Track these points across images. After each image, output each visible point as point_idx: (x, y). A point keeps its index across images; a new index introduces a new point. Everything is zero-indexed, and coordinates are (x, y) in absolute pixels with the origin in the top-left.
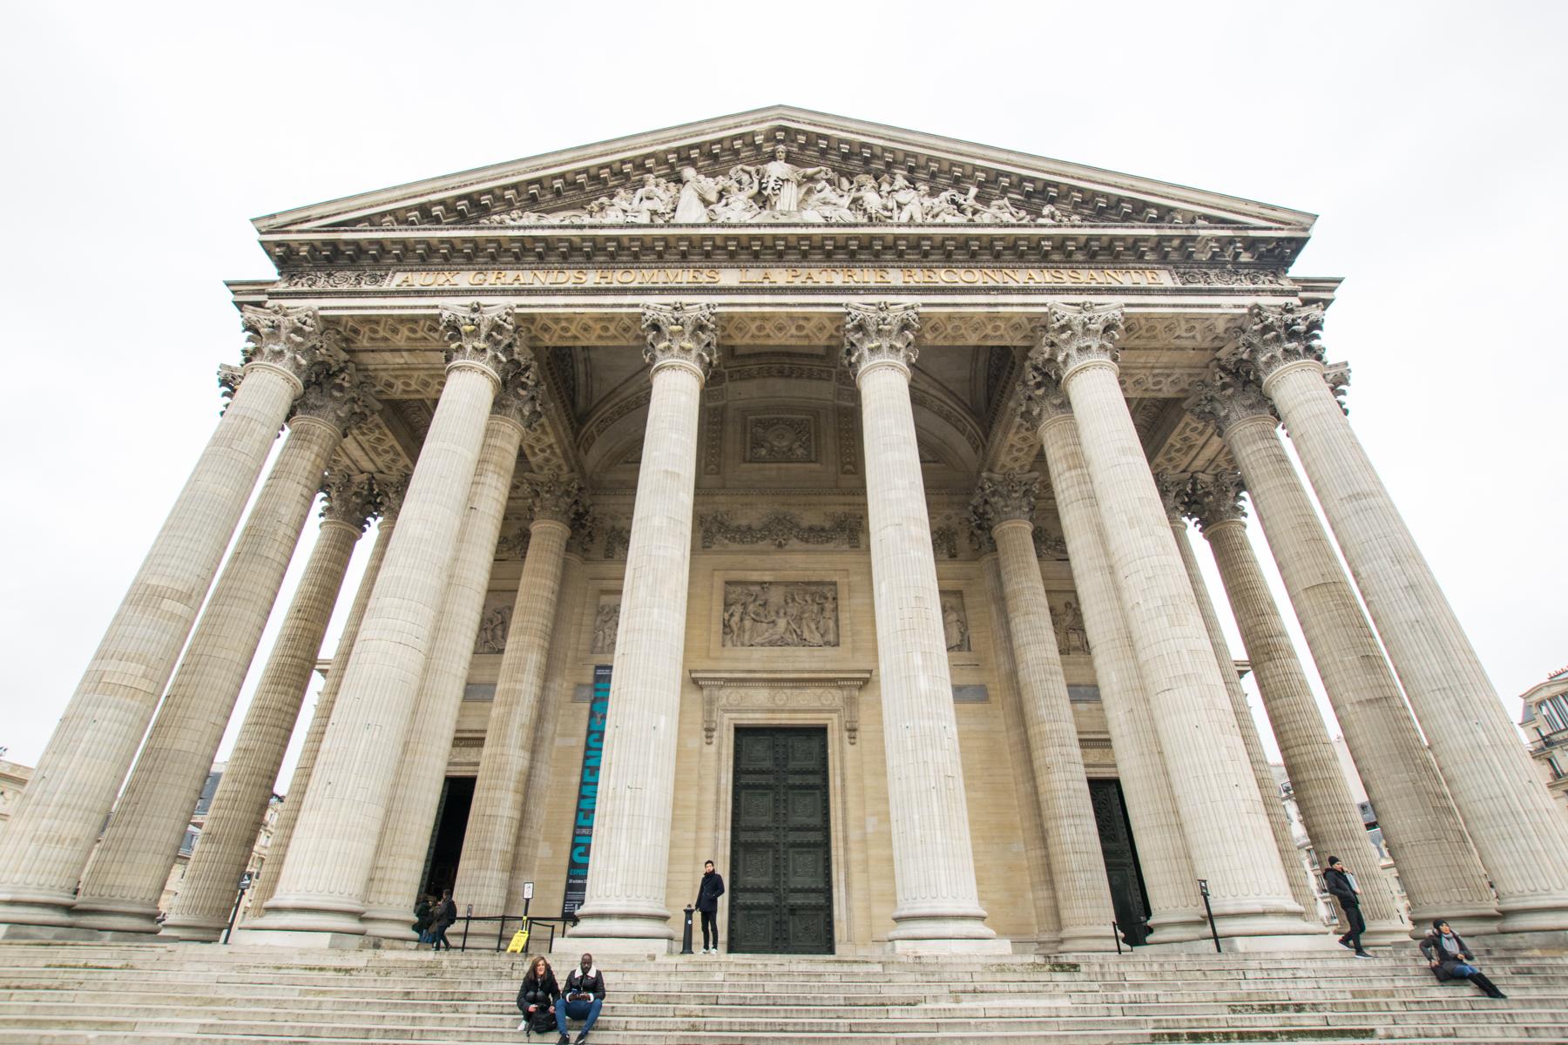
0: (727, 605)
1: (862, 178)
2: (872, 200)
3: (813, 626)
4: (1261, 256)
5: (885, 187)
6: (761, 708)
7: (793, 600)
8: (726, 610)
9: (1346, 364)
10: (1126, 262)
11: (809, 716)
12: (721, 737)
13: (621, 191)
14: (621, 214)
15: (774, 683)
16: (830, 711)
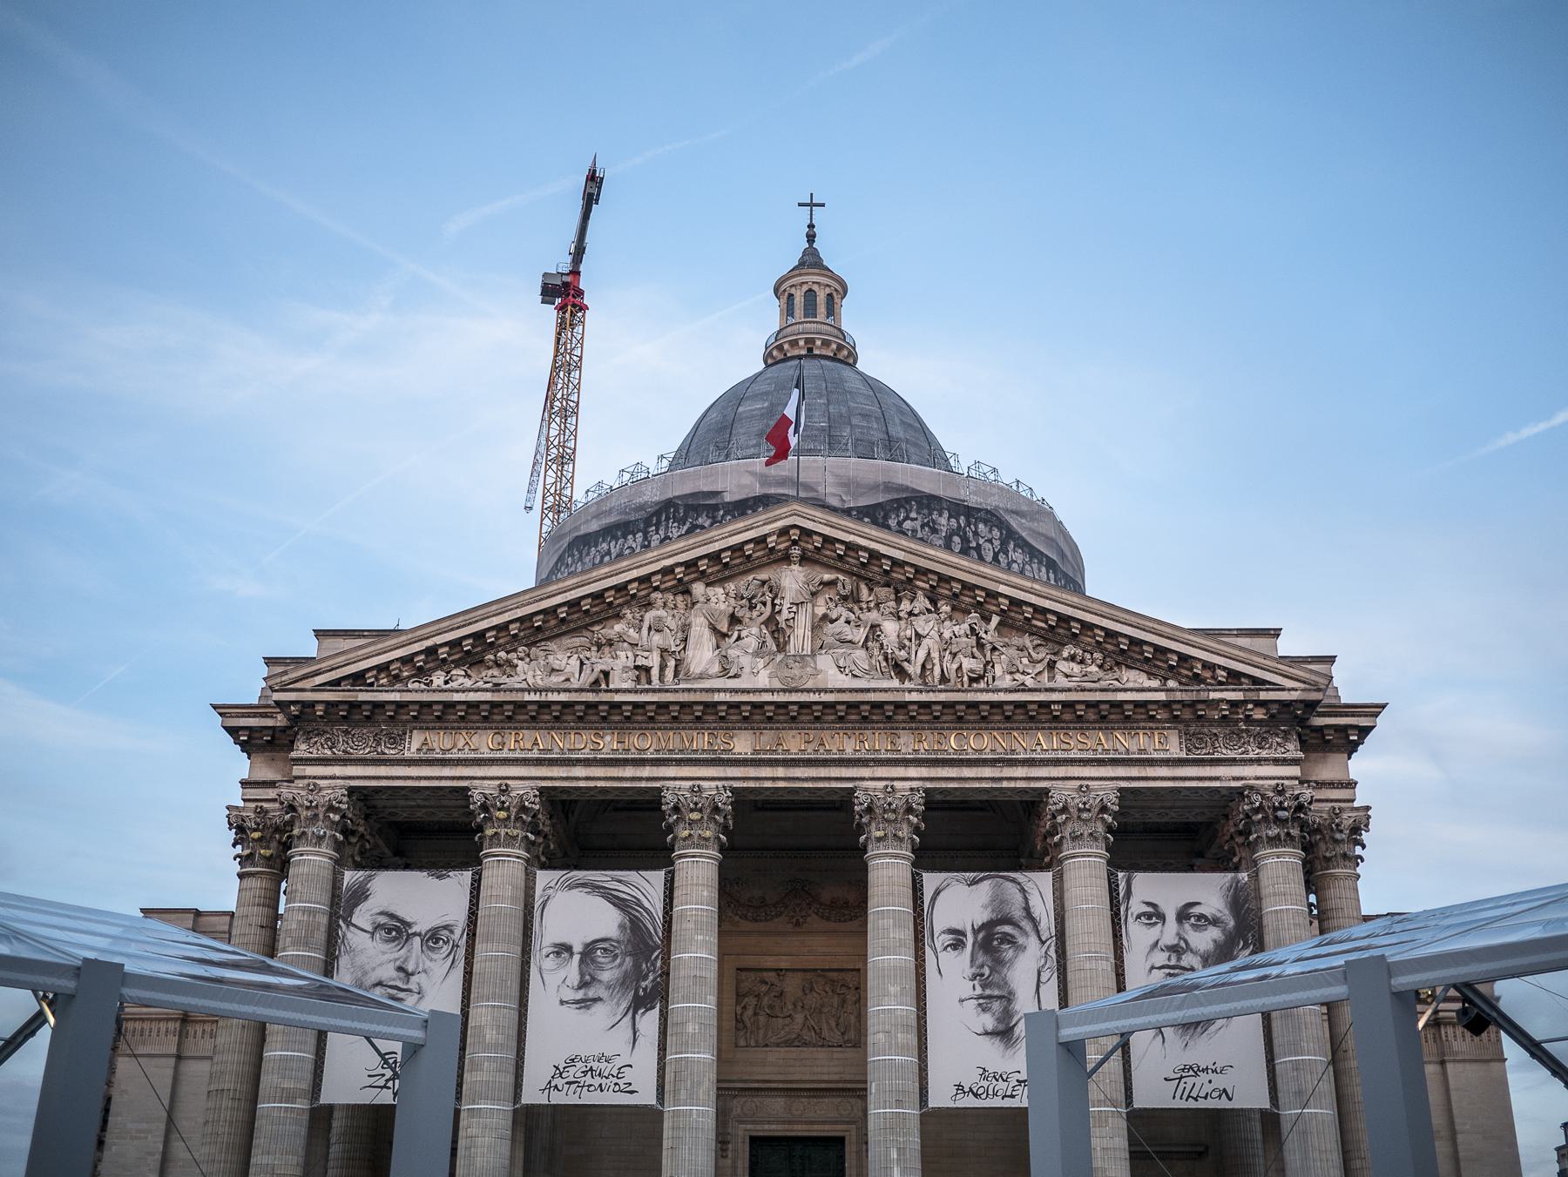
0: (740, 996)
1: (883, 592)
2: (890, 628)
3: (833, 1024)
4: (1272, 716)
5: (906, 606)
6: (776, 1117)
7: (812, 989)
8: (738, 1003)
9: (1368, 808)
10: (1137, 721)
11: (827, 1127)
12: (735, 1150)
13: (627, 611)
14: (630, 654)
15: (791, 1092)
16: (848, 1123)
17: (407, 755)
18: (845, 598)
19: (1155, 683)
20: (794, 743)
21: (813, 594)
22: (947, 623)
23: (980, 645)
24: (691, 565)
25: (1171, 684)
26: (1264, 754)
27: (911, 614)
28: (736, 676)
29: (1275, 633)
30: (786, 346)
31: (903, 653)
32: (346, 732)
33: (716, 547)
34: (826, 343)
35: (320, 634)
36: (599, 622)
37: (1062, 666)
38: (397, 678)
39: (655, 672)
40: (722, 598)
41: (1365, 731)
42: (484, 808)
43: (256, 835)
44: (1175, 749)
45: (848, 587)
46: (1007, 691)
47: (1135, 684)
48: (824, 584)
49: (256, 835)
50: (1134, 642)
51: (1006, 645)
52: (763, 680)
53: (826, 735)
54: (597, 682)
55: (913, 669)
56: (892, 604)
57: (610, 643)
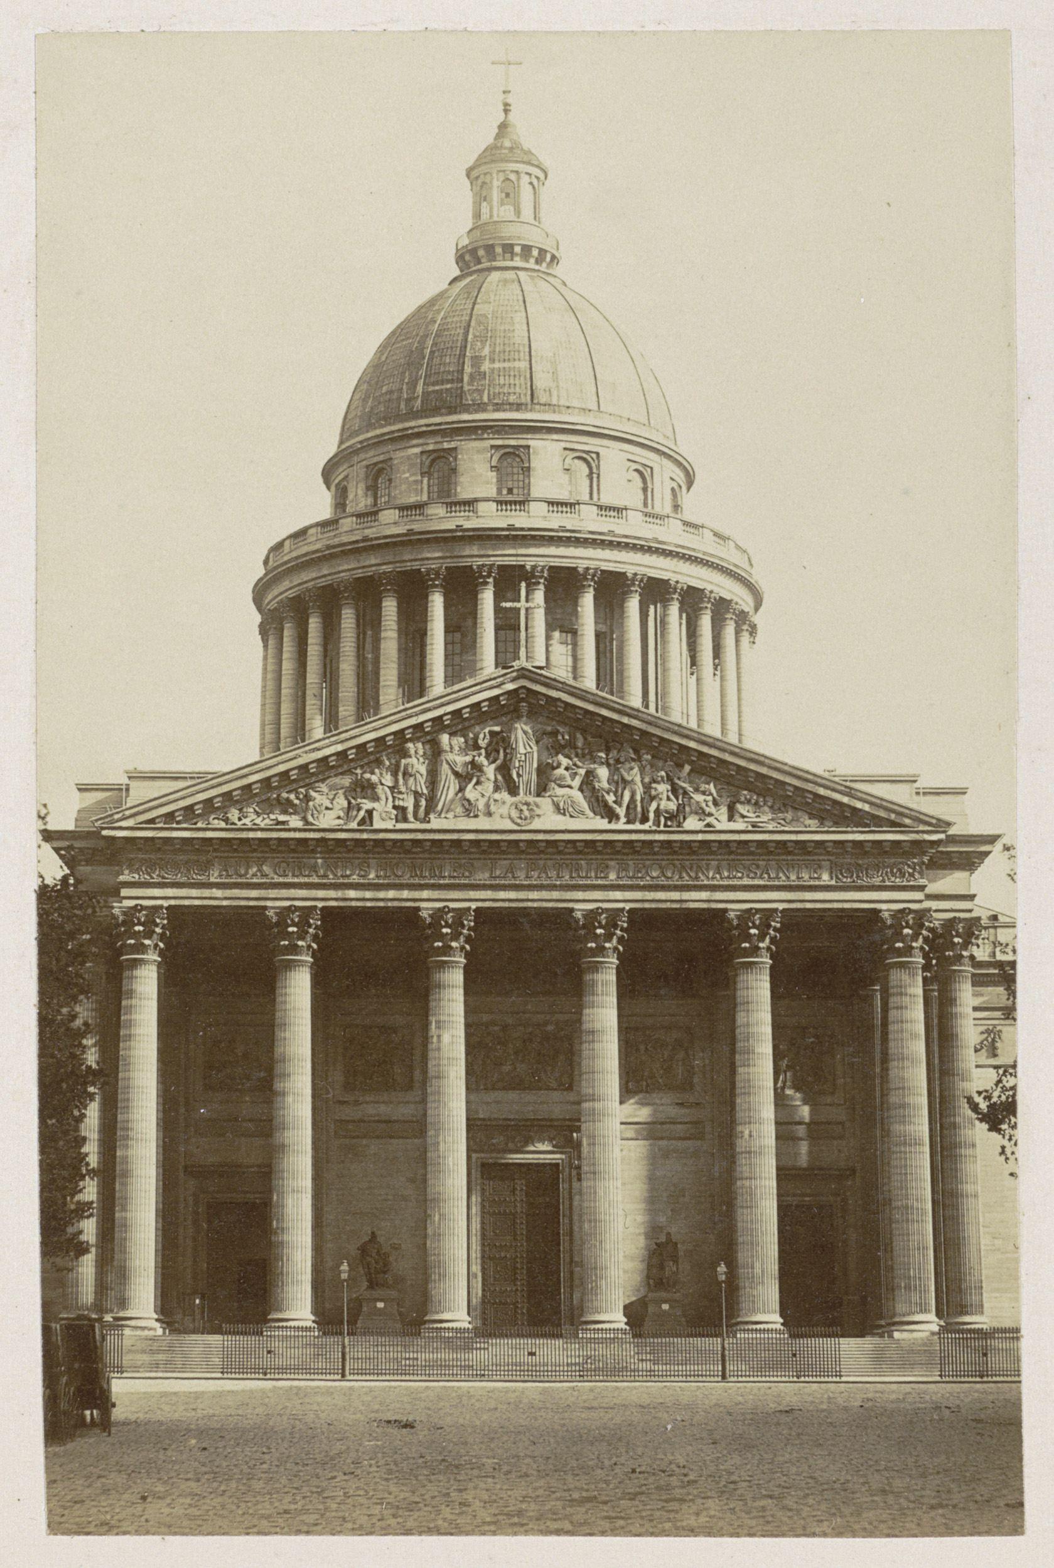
5: (614, 754)
17: (212, 880)
19: (813, 824)
27: (618, 761)
28: (476, 816)
39: (411, 809)
51: (697, 790)
54: (363, 818)
55: (621, 811)
57: (372, 786)
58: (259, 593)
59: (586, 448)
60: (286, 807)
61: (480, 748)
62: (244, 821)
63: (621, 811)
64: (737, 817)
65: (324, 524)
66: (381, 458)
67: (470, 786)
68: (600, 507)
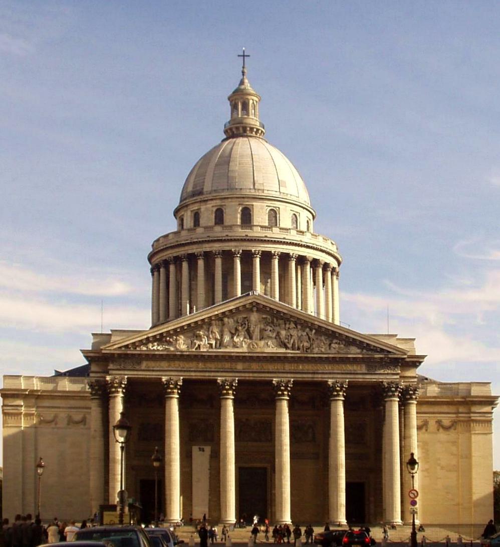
1: (281, 322)
2: (283, 333)
5: (287, 326)
14: (206, 339)
18: (269, 323)
19: (359, 351)
20: (255, 366)
21: (260, 321)
22: (300, 331)
23: (309, 338)
24: (223, 313)
25: (365, 351)
26: (389, 372)
27: (289, 328)
29: (396, 335)
30: (234, 130)
31: (287, 340)
32: (124, 361)
33: (231, 308)
34: (252, 129)
35: (112, 331)
36: (196, 329)
37: (333, 345)
38: (137, 346)
40: (233, 322)
41: (420, 363)
42: (166, 384)
43: (96, 388)
44: (364, 371)
45: (271, 320)
46: (317, 354)
47: (354, 352)
48: (263, 318)
49: (96, 388)
50: (353, 339)
51: (317, 339)
52: (244, 349)
53: (264, 364)
55: (290, 346)
56: (284, 326)
58: (150, 258)
59: (274, 205)
60: (169, 343)
61: (239, 323)
62: (155, 348)
63: (290, 346)
64: (332, 349)
65: (175, 233)
66: (196, 208)
67: (235, 337)
68: (281, 229)
